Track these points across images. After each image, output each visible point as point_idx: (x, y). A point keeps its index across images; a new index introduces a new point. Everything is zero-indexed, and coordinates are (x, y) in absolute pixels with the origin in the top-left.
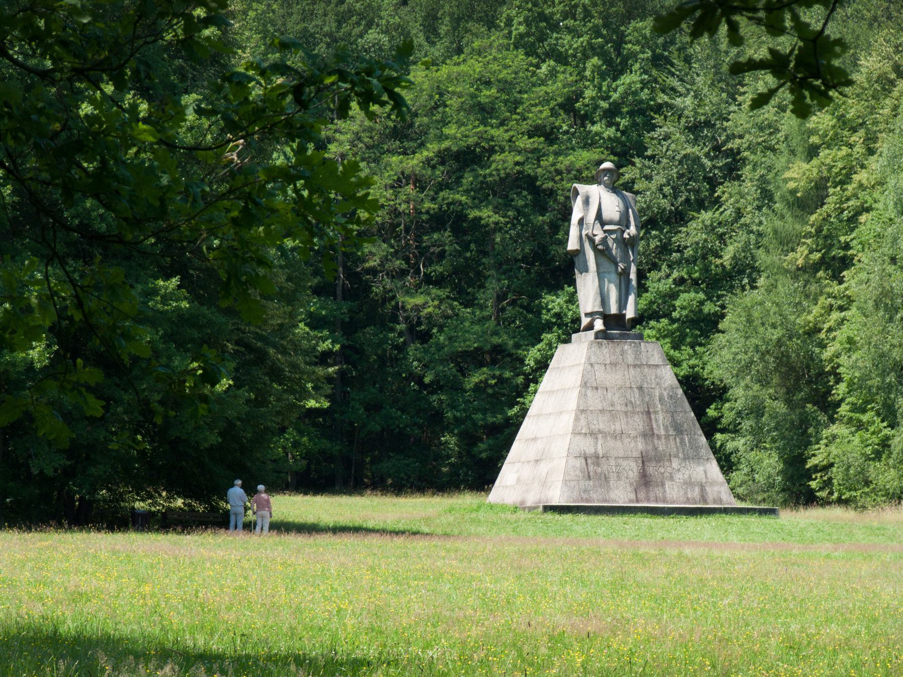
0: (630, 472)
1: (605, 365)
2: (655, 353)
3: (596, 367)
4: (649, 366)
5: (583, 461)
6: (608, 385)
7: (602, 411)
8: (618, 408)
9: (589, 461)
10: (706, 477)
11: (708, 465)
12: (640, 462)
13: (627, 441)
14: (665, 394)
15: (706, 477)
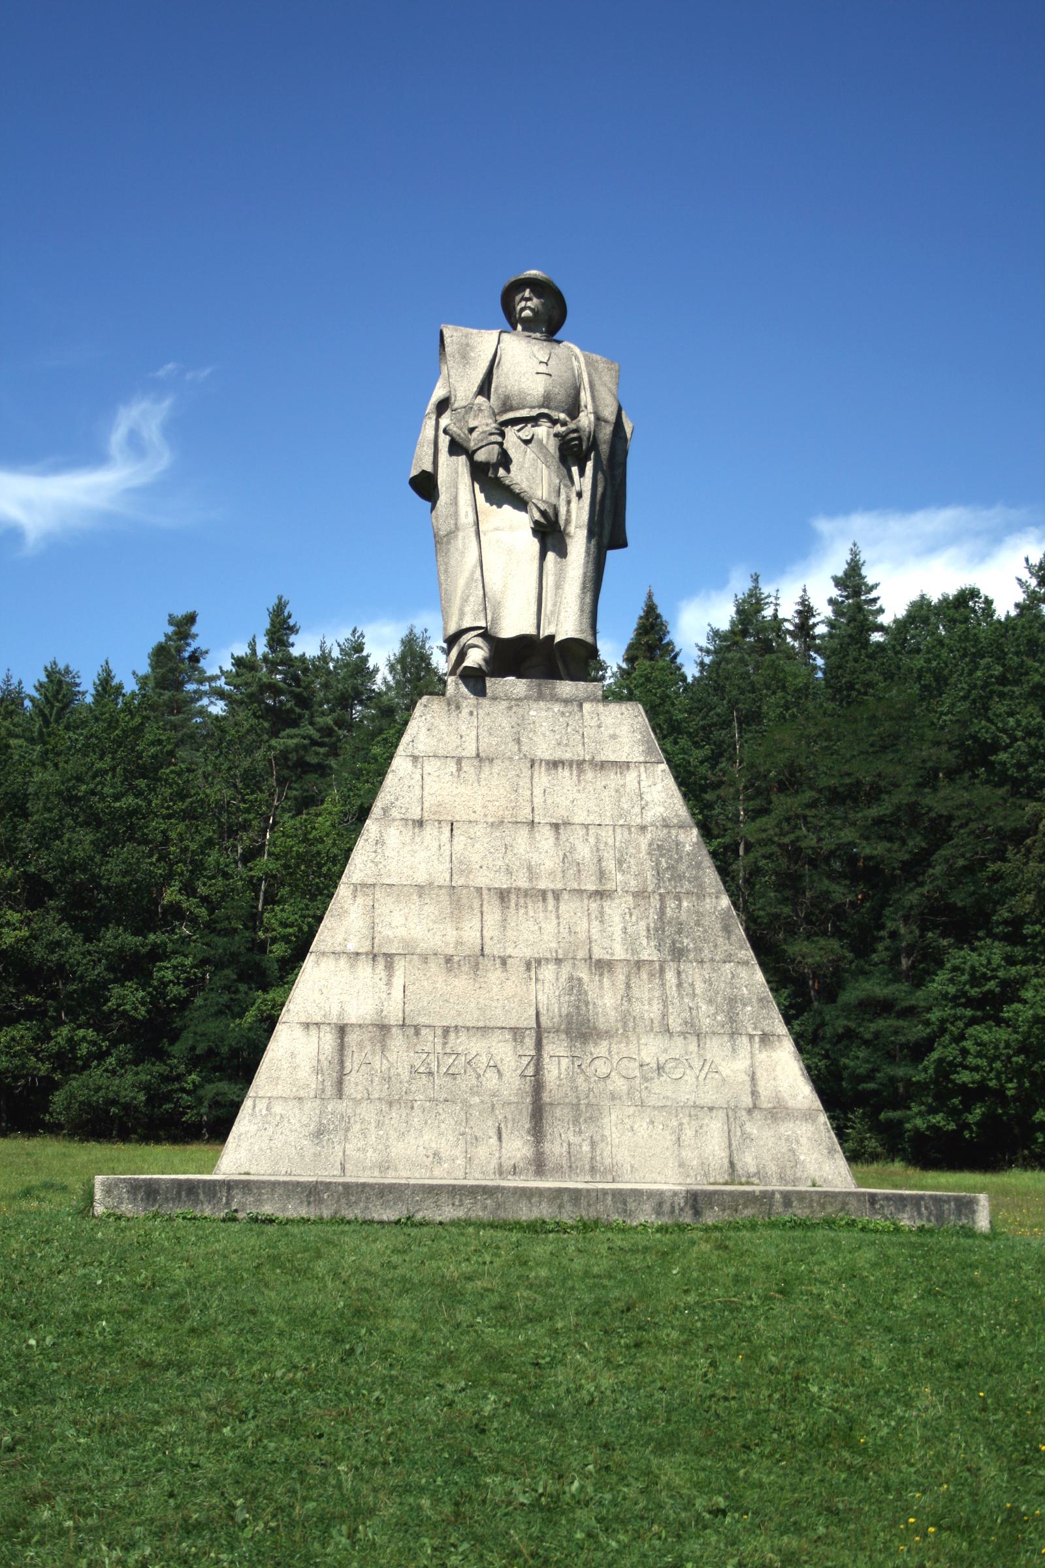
0: (491, 1075)
1: (459, 761)
2: (624, 731)
3: (430, 766)
4: (603, 766)
5: (329, 1040)
6: (461, 815)
7: (421, 889)
8: (483, 879)
9: (352, 1038)
10: (754, 1094)
11: (762, 1056)
12: (530, 1042)
13: (495, 976)
14: (644, 841)
15: (754, 1094)
